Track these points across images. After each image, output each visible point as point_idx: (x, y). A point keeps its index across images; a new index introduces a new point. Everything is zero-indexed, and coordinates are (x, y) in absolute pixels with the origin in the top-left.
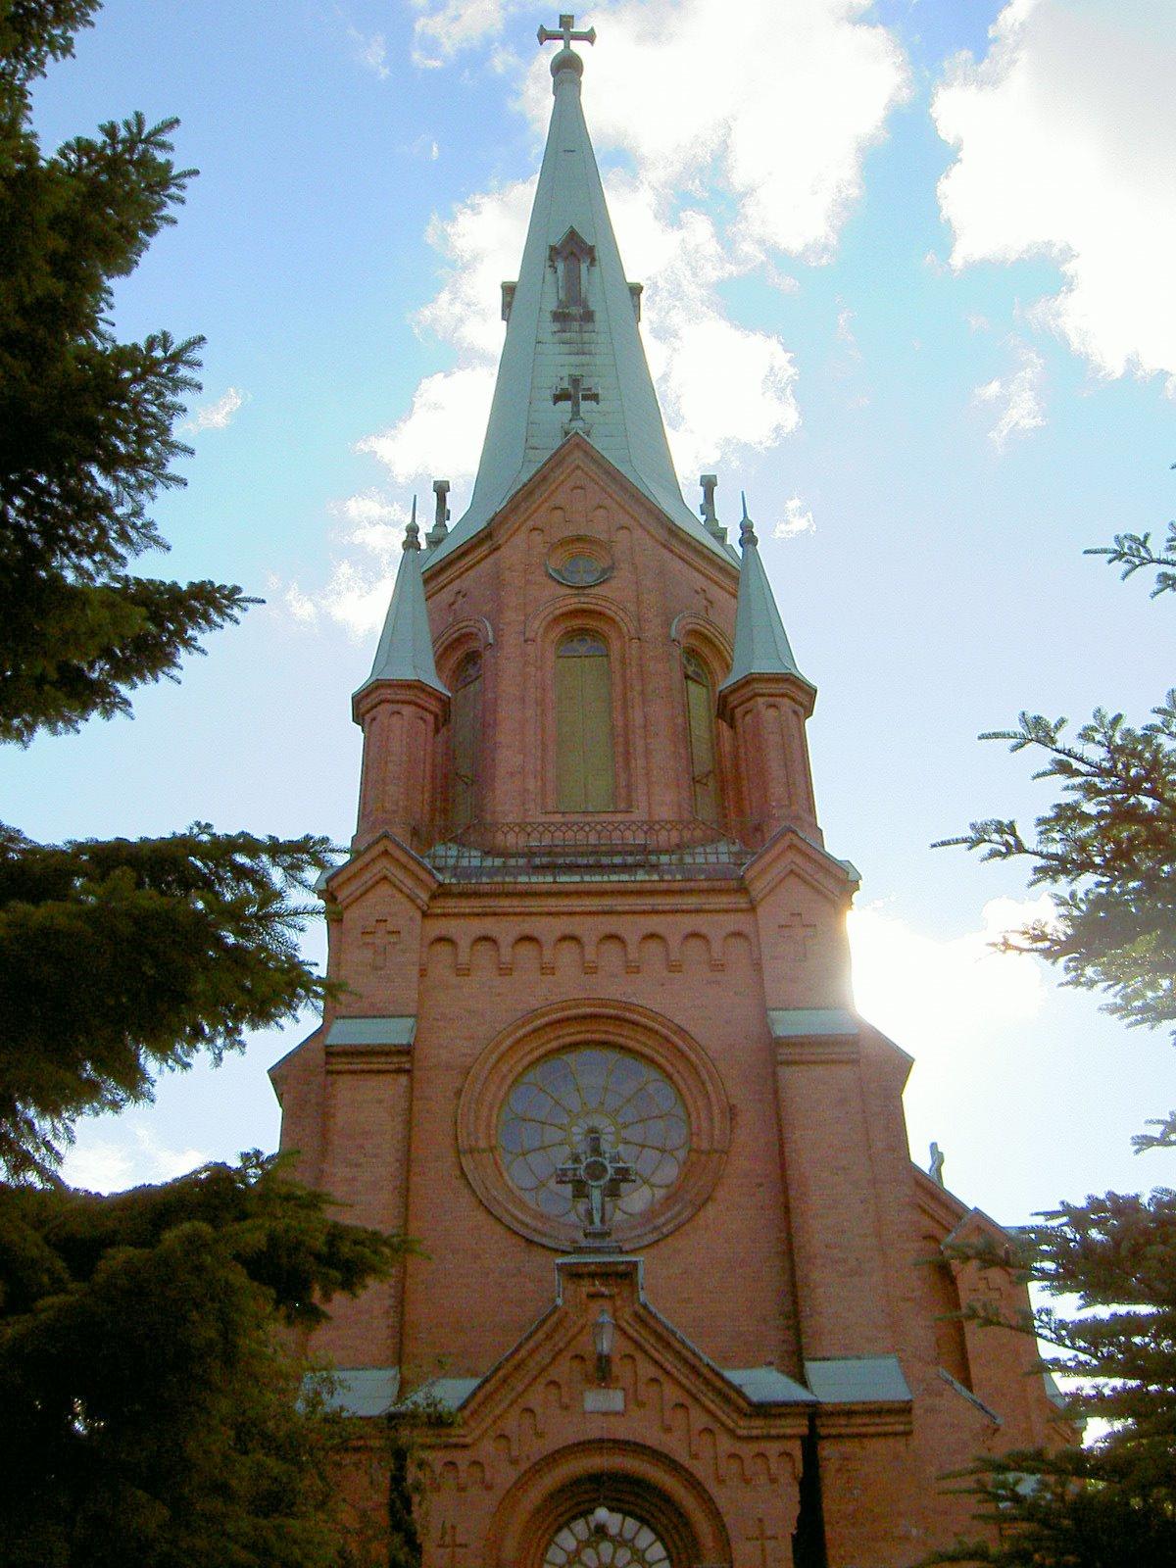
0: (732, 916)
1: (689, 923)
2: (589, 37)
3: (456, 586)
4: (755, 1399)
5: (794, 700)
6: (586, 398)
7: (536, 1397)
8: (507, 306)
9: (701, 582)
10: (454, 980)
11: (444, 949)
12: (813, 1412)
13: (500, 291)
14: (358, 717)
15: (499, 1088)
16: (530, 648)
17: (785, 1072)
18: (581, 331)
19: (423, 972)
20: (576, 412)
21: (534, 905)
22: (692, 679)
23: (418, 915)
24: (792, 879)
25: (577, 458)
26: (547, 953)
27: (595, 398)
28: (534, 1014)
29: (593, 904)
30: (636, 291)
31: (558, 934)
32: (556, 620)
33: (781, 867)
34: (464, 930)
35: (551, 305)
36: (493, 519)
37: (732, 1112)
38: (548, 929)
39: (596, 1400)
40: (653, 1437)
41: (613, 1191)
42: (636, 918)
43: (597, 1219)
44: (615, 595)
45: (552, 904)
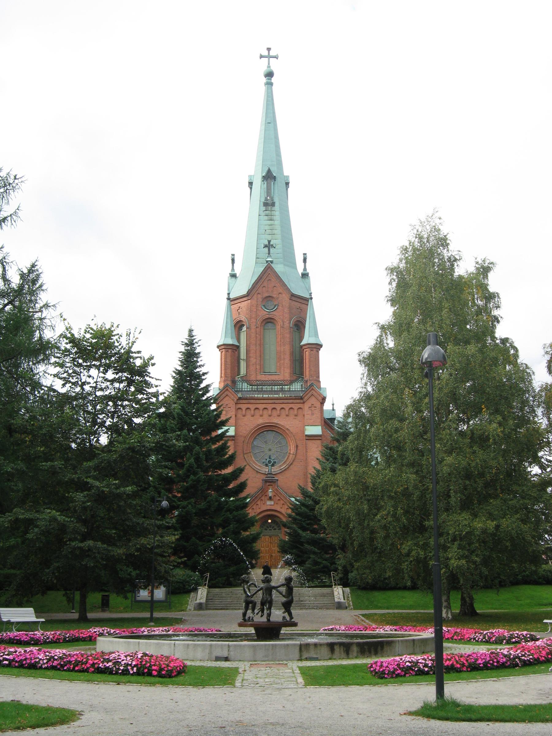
2: (276, 57)
7: (259, 503)
9: (298, 305)
11: (239, 411)
13: (248, 183)
16: (257, 329)
19: (236, 416)
20: (269, 254)
21: (258, 401)
25: (269, 271)
28: (259, 425)
30: (287, 184)
34: (244, 407)
37: (297, 446)
38: (261, 407)
39: (269, 503)
41: (273, 465)
44: (277, 315)
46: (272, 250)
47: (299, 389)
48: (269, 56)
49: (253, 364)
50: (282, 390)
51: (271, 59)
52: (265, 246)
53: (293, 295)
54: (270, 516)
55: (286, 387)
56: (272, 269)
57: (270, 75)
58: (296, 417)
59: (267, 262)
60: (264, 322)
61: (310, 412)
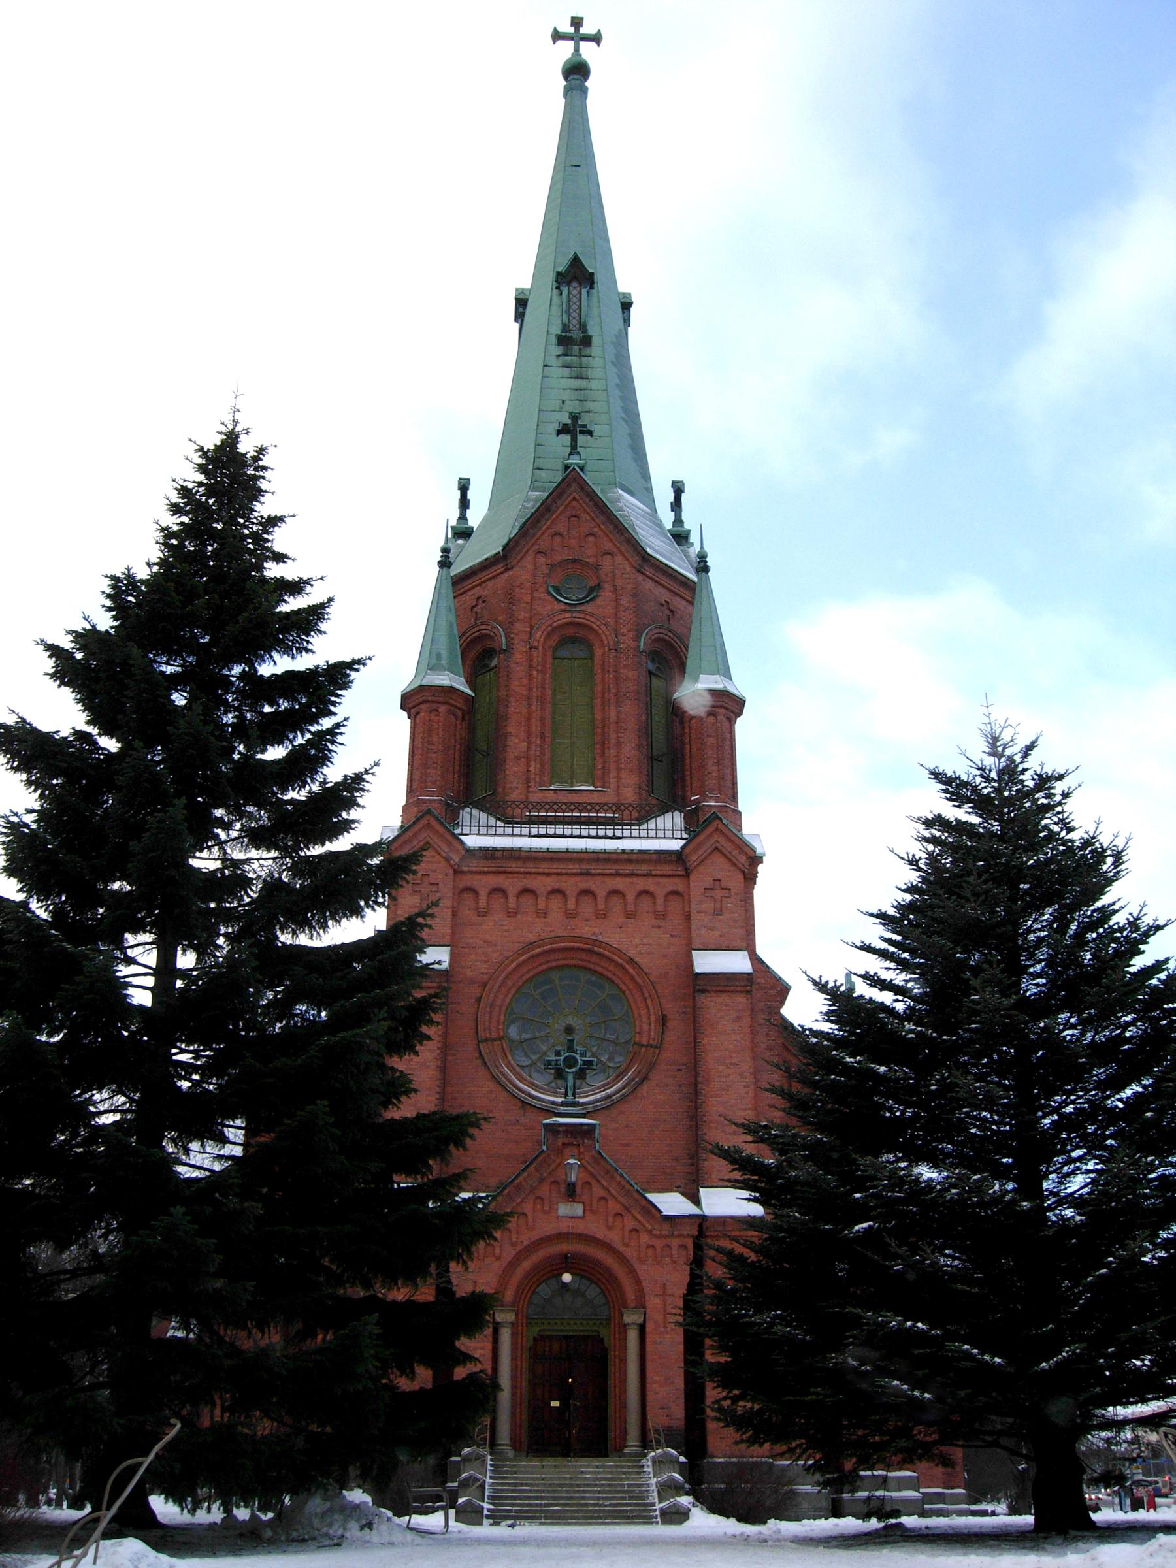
0: (671, 880)
1: (642, 884)
2: (596, 39)
3: (477, 591)
4: (665, 1213)
5: (727, 709)
6: (582, 432)
8: (520, 316)
9: (664, 596)
10: (475, 918)
11: (468, 898)
12: (702, 1221)
13: (514, 302)
14: (403, 707)
15: (506, 996)
17: (701, 999)
18: (580, 356)
19: (454, 914)
20: (574, 447)
22: (656, 675)
23: (451, 872)
24: (717, 854)
26: (542, 903)
27: (590, 433)
30: (626, 306)
31: (550, 888)
32: (554, 630)
33: (708, 846)
35: (556, 330)
36: (507, 544)
37: (664, 1020)
38: (542, 884)
39: (564, 1209)
40: (600, 1233)
42: (606, 879)
43: (570, 1093)
46: (581, 439)
48: (576, 32)
49: (518, 758)
51: (582, 44)
52: (563, 430)
53: (646, 558)
54: (567, 1262)
56: (583, 486)
57: (576, 72)
58: (659, 923)
59: (567, 467)
60: (556, 638)
61: (708, 905)
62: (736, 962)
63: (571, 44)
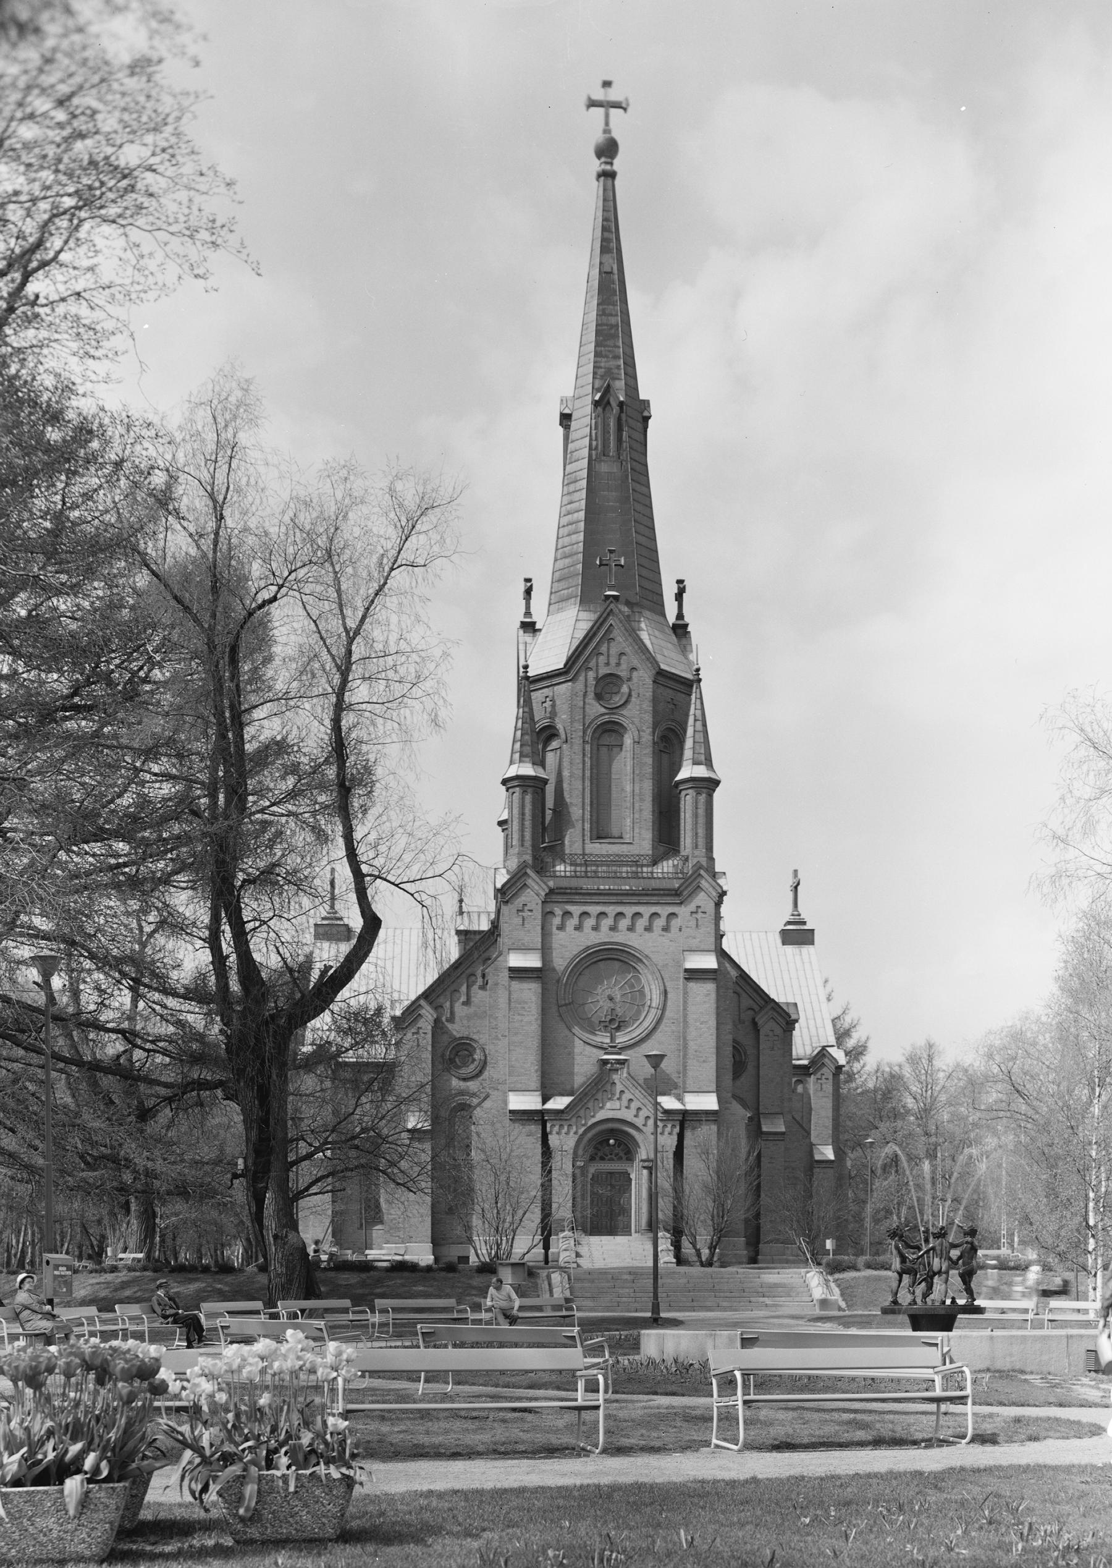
28: (588, 948)
29: (613, 899)
45: (595, 899)
47: (670, 876)
50: (636, 876)
55: (645, 869)
57: (608, 149)
60: (600, 731)
62: (709, 962)
63: (601, 110)
